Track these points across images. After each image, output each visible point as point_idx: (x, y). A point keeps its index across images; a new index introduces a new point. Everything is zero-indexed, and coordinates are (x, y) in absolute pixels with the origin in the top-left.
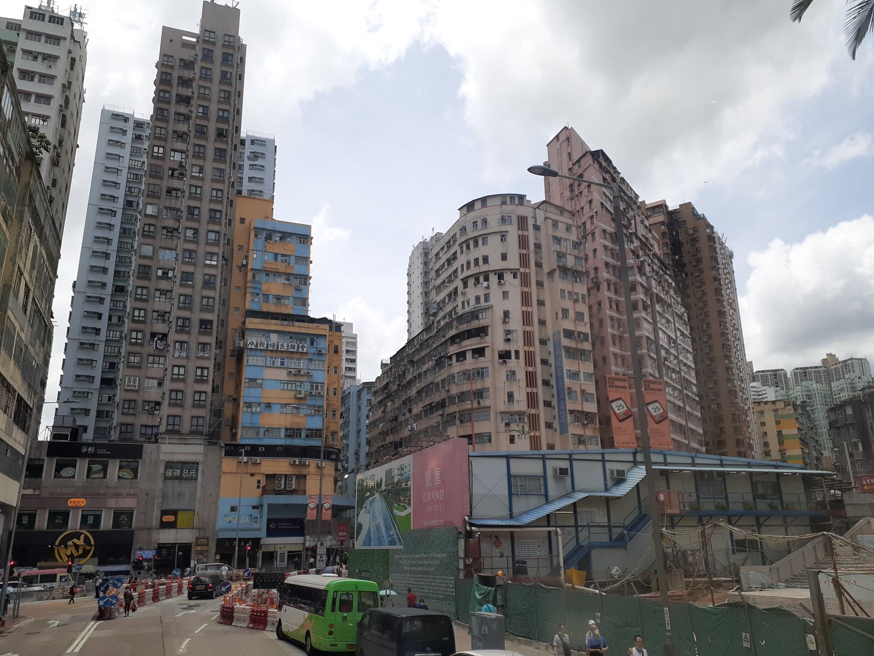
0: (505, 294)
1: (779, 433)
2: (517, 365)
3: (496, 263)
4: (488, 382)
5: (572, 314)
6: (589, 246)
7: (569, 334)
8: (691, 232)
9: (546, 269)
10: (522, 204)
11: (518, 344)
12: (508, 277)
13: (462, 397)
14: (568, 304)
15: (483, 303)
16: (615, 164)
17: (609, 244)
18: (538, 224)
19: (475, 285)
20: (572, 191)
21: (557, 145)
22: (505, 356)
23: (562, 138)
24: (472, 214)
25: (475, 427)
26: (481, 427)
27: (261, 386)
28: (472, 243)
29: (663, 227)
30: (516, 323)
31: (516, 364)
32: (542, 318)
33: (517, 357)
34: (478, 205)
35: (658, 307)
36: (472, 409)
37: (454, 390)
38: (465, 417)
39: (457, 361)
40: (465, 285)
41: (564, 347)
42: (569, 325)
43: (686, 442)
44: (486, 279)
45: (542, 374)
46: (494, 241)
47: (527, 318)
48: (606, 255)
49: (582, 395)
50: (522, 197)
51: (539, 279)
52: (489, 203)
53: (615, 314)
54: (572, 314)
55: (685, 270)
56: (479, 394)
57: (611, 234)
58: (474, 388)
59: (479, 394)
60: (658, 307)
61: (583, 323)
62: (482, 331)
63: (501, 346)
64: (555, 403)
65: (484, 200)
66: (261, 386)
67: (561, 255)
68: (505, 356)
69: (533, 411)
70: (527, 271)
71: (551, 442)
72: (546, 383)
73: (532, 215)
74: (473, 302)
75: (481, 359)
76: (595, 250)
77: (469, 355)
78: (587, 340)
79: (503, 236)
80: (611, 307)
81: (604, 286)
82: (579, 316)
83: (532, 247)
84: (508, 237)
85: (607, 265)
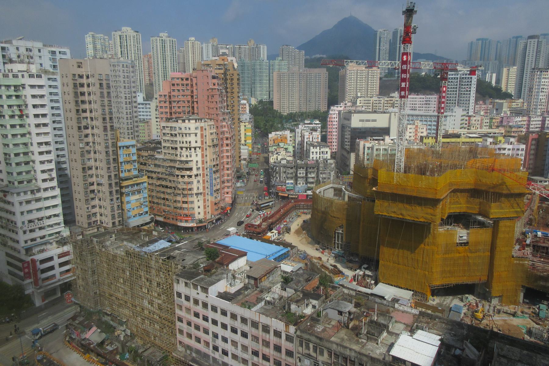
0: (197, 155)
1: (245, 134)
2: (200, 178)
3: (193, 145)
11: (201, 172)
12: (197, 149)
13: (183, 189)
26: (190, 199)
27: (130, 203)
30: (200, 165)
38: (185, 196)
44: (190, 149)
46: (193, 136)
47: (203, 162)
62: (190, 169)
66: (130, 203)
68: (197, 175)
79: (196, 136)
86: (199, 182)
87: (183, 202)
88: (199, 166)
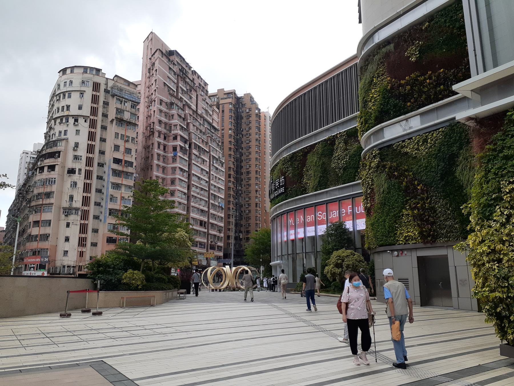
0: (78, 132)
3: (74, 111)
4: (54, 188)
5: (122, 149)
6: (153, 108)
7: (117, 161)
8: (248, 111)
9: (110, 118)
10: (98, 75)
11: (81, 165)
12: (81, 121)
14: (120, 142)
15: (63, 137)
16: (187, 61)
17: (164, 109)
18: (109, 89)
19: (60, 123)
20: (149, 73)
21: (147, 42)
22: (72, 171)
23: (150, 38)
24: (65, 77)
25: (42, 215)
26: (46, 216)
28: (62, 95)
29: (230, 106)
30: (82, 152)
31: (78, 178)
32: (102, 149)
33: (80, 173)
34: (68, 71)
35: (194, 151)
36: (42, 205)
37: (36, 192)
38: (38, 209)
39: (39, 173)
40: (55, 122)
41: (112, 169)
42: (119, 156)
43: (206, 230)
45: (97, 185)
46: (75, 96)
47: (90, 149)
48: (161, 116)
49: (121, 200)
50: (98, 70)
51: (104, 124)
52: (76, 70)
53: (162, 153)
54: (122, 149)
55: (243, 133)
56: (48, 195)
57: (166, 103)
58: (45, 191)
59: (48, 195)
60: (194, 151)
61: (130, 156)
63: (70, 164)
64: (103, 204)
65: (72, 68)
67: (119, 111)
68: (72, 171)
69: (86, 208)
70: (95, 118)
71: (96, 227)
72: (99, 191)
73: (105, 83)
74: (57, 135)
75: (52, 172)
76: (154, 111)
77: (46, 169)
78: (132, 166)
80: (159, 147)
81: (156, 134)
82: (128, 151)
83: (101, 103)
84: (85, 95)
85: (160, 122)
86: (75, 184)
87: (37, 223)
88: (78, 153)
